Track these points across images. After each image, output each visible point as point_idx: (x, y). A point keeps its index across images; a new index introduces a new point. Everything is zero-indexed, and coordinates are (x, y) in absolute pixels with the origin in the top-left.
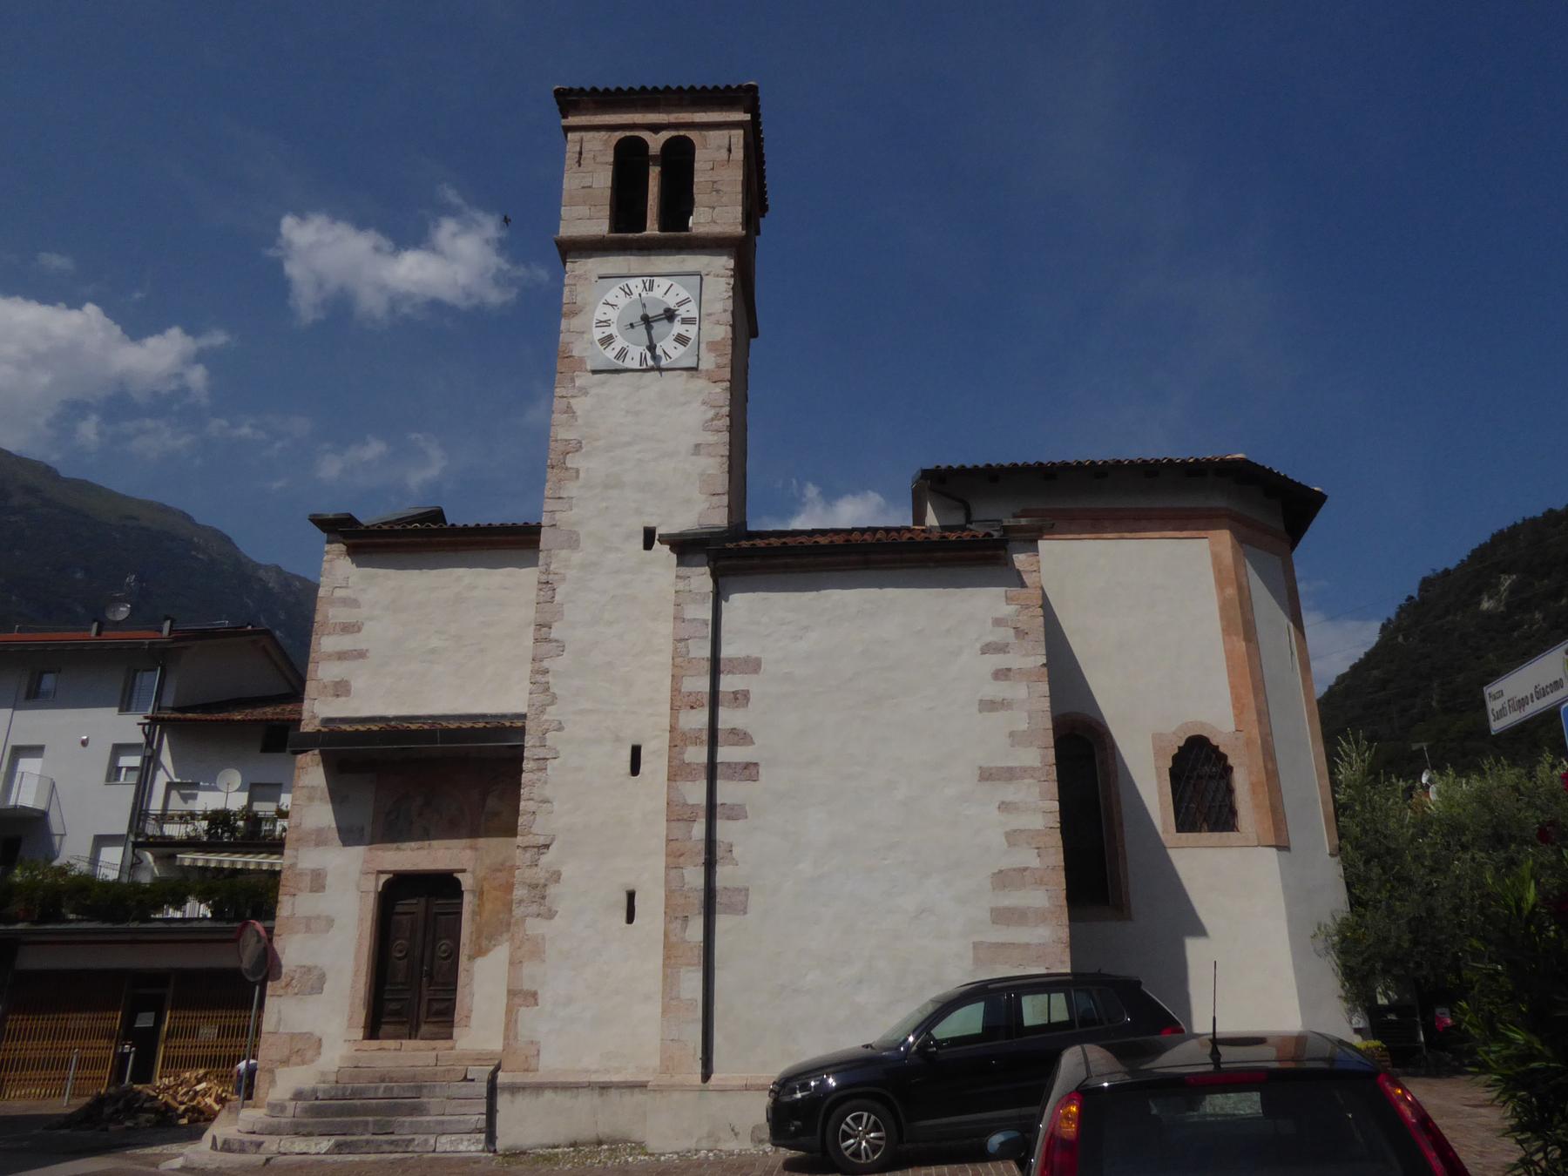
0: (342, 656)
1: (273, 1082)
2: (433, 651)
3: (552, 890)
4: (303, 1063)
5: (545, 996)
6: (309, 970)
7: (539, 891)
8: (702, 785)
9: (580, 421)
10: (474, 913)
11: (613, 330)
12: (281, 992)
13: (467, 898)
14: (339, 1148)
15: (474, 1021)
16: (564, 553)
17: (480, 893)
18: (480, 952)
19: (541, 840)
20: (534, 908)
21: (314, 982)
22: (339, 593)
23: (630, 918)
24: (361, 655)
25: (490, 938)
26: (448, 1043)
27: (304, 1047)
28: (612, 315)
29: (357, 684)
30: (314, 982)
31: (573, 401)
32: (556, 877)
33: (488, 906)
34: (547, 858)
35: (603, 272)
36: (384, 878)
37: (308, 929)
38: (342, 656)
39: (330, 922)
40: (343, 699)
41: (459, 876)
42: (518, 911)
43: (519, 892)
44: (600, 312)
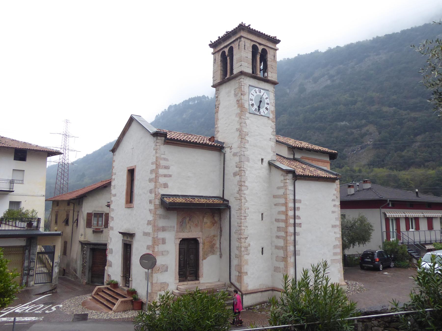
0: (165, 176)
2: (189, 177)
3: (249, 248)
5: (249, 273)
7: (246, 248)
8: (293, 228)
9: (248, 127)
10: (203, 249)
11: (253, 102)
12: (157, 272)
16: (247, 163)
17: (204, 244)
18: (204, 258)
19: (246, 236)
20: (246, 253)
21: (165, 269)
22: (163, 156)
23: (262, 254)
24: (170, 176)
25: (207, 255)
26: (197, 282)
28: (253, 98)
29: (170, 185)
30: (165, 269)
32: (249, 245)
33: (206, 247)
34: (247, 241)
35: (251, 84)
36: (180, 240)
37: (163, 255)
38: (165, 176)
39: (168, 252)
41: (198, 239)
42: (243, 253)
43: (243, 249)
44: (251, 97)
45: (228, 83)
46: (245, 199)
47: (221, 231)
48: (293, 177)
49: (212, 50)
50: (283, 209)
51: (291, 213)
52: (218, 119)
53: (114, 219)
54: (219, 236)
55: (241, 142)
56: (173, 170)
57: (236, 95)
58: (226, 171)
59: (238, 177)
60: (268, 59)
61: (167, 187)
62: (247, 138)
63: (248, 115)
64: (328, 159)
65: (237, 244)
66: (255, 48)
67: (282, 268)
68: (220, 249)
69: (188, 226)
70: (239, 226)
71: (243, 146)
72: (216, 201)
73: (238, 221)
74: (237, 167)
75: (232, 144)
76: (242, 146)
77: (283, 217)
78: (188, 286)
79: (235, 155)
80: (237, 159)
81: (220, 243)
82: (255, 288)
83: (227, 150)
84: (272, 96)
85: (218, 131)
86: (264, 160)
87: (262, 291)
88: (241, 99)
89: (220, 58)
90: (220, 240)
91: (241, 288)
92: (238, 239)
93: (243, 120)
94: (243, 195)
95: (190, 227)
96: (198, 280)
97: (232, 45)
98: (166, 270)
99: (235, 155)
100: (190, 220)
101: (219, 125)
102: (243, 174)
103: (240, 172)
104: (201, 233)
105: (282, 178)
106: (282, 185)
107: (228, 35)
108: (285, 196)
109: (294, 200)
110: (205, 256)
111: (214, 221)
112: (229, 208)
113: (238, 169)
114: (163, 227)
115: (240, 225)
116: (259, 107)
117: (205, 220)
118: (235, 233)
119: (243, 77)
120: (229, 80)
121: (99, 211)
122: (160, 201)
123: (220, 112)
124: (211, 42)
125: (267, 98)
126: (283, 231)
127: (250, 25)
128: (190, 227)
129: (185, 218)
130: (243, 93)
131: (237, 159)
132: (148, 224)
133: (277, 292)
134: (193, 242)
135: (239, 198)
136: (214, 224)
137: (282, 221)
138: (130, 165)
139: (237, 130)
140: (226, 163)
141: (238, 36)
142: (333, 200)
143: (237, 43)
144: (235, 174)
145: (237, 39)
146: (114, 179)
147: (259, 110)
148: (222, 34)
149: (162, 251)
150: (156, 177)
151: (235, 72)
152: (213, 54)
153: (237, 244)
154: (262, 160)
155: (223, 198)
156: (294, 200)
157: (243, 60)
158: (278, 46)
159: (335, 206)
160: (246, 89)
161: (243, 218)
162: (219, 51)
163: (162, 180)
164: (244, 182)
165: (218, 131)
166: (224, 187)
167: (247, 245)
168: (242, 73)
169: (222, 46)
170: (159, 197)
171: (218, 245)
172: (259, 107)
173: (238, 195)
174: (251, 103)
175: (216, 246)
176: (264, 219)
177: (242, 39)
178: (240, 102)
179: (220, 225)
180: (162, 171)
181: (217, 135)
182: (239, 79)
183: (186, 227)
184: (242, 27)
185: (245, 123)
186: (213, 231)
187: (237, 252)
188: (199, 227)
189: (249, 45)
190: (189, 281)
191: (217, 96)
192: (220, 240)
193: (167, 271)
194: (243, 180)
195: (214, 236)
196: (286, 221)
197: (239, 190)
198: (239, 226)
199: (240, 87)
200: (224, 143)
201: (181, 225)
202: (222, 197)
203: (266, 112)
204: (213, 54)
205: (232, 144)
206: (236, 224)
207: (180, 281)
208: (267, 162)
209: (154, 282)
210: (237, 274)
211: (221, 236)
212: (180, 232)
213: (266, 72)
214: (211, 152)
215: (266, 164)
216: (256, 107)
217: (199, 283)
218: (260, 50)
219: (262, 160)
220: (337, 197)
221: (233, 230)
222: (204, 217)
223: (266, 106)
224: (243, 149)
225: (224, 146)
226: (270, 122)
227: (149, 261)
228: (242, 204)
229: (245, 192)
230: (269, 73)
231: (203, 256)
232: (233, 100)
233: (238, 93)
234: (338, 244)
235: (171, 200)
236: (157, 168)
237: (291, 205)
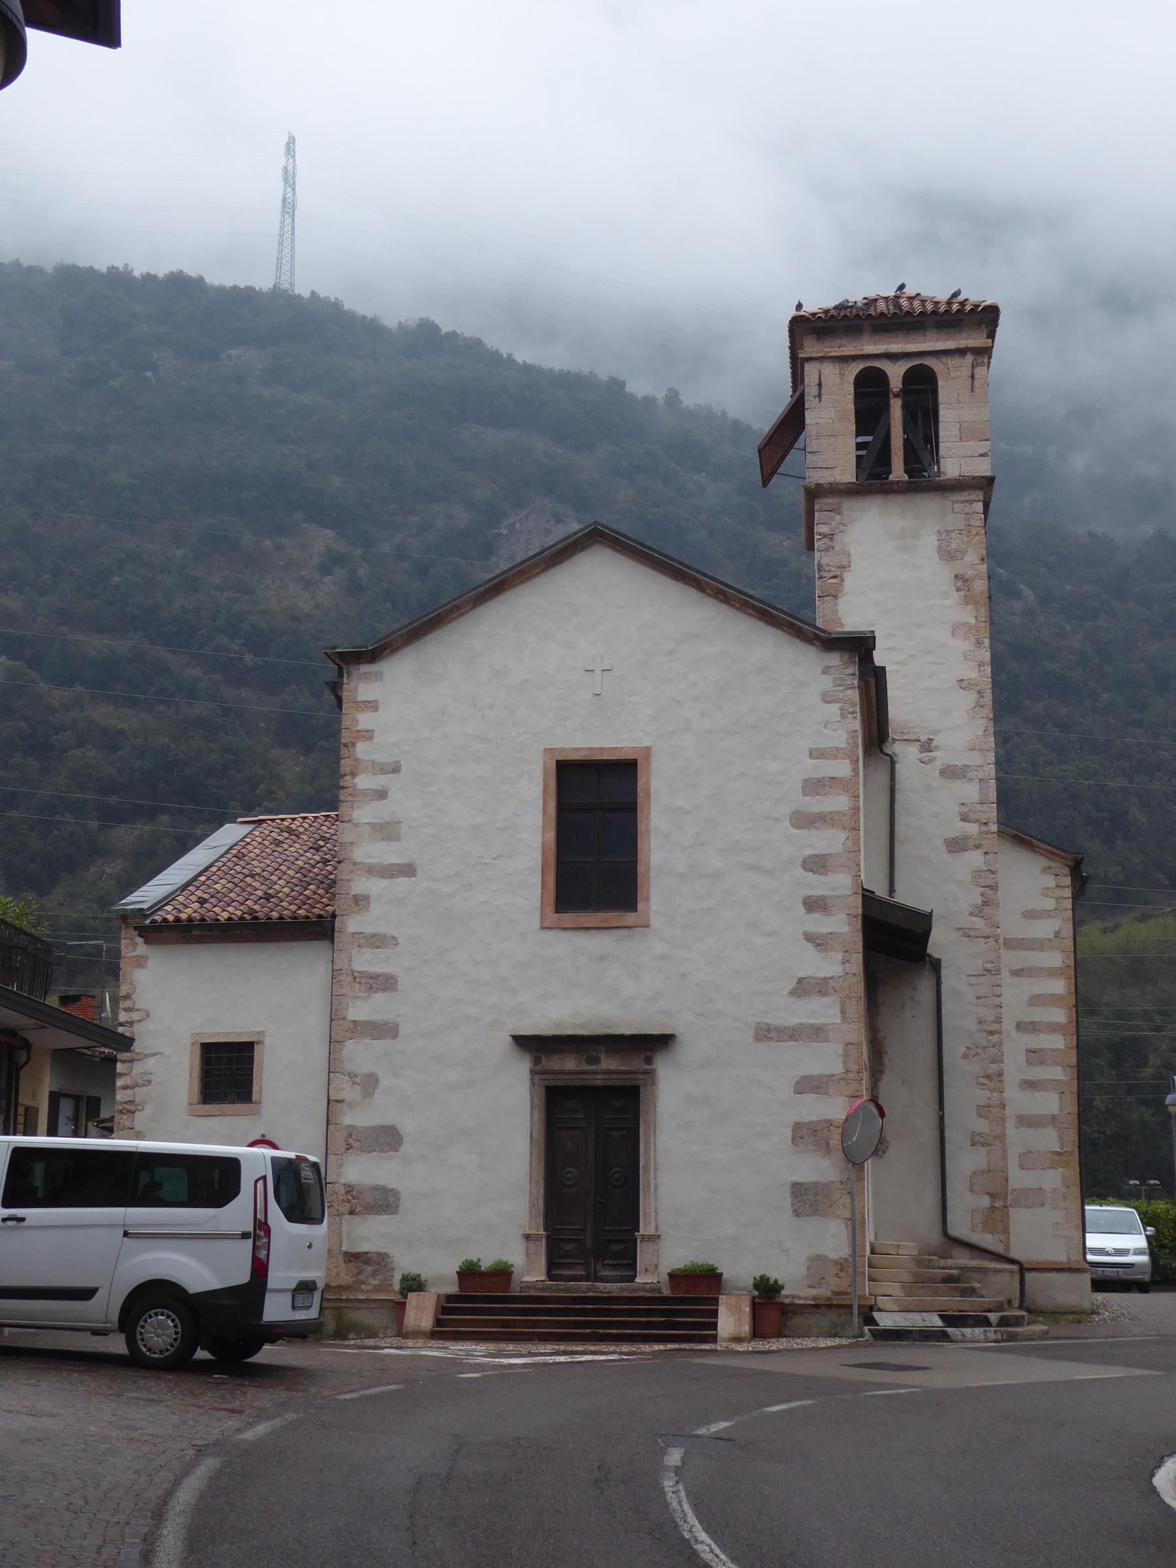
65: (982, 1096)
67: (1054, 1190)
70: (991, 1033)
74: (965, 818)
91: (1007, 1246)
92: (988, 1077)
99: (951, 773)
113: (973, 829)
115: (995, 1027)
126: (1055, 1063)
135: (987, 931)
153: (982, 1096)
173: (979, 923)
197: (986, 903)
198: (991, 1033)
206: (971, 1025)
210: (986, 1201)
221: (954, 1048)
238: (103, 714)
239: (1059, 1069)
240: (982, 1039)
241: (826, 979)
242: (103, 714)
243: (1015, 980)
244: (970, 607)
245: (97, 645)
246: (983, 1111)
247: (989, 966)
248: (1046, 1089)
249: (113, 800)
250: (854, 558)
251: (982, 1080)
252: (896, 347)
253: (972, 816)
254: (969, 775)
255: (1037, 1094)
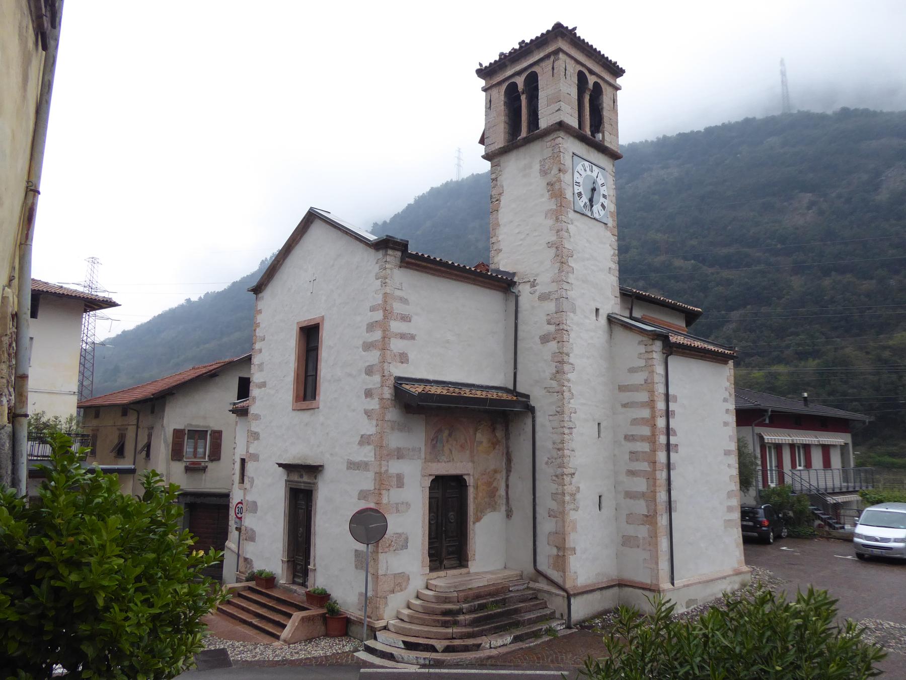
0: (403, 336)
1: (386, 604)
2: (448, 342)
3: (578, 496)
4: (402, 590)
6: (400, 535)
7: (573, 495)
9: (572, 240)
10: (475, 498)
11: (581, 189)
12: (387, 550)
13: (471, 492)
14: (517, 639)
15: (477, 557)
16: (572, 315)
17: (476, 487)
18: (478, 519)
20: (572, 506)
22: (398, 293)
24: (413, 337)
25: (482, 512)
26: (463, 571)
27: (401, 581)
28: (580, 180)
29: (411, 356)
30: (403, 543)
31: (570, 226)
34: (574, 480)
37: (398, 511)
38: (403, 336)
39: (408, 505)
40: (405, 365)
41: (466, 477)
42: (568, 507)
43: (567, 498)
45: (522, 151)
46: (570, 391)
47: (509, 460)
48: (664, 348)
49: (482, 83)
50: (646, 413)
51: (661, 423)
52: (498, 225)
53: (261, 436)
54: (504, 472)
55: (560, 270)
56: (419, 325)
57: (544, 172)
58: (520, 333)
59: (553, 345)
60: (605, 105)
61: (407, 361)
62: (571, 262)
63: (571, 215)
64: (684, 325)
65: (553, 487)
66: (582, 79)
67: (644, 538)
68: (507, 498)
69: (446, 449)
70: (559, 450)
71: (564, 278)
72: (505, 396)
73: (557, 438)
74: (549, 324)
75: (537, 275)
76: (560, 280)
77: (646, 431)
78: (447, 580)
79: (544, 297)
80: (551, 307)
81: (507, 486)
82: (589, 582)
83: (524, 290)
84: (611, 181)
85: (499, 251)
86: (601, 311)
87: (601, 589)
88: (559, 180)
89: (502, 98)
90: (507, 479)
91: (564, 581)
92: (557, 476)
93: (564, 224)
94: (566, 383)
95: (451, 451)
96: (467, 566)
97: (536, 69)
98: (405, 546)
99: (544, 297)
100: (450, 435)
101: (500, 238)
102: (565, 338)
103: (557, 333)
104: (470, 464)
105: (642, 349)
106: (642, 363)
107: (525, 49)
108: (649, 385)
109: (667, 395)
110: (479, 514)
111: (495, 440)
112: (531, 410)
113: (552, 328)
114: (399, 450)
115: (560, 446)
116: (591, 200)
117: (479, 435)
118: (547, 463)
119: (562, 134)
120: (527, 141)
121: (198, 426)
122: (391, 391)
123: (502, 211)
124: (481, 65)
125: (603, 185)
126: (645, 460)
127: (575, 29)
128: (451, 451)
129: (440, 431)
130: (562, 167)
131: (551, 307)
132: (361, 443)
133: (631, 589)
134: (453, 484)
136: (494, 444)
137: (643, 439)
138: (308, 317)
139: (550, 245)
140: (520, 316)
141: (551, 49)
142: (725, 400)
143: (548, 64)
144: (545, 339)
145: (547, 57)
146: (260, 351)
147: (592, 206)
148: (510, 45)
149: (397, 504)
150: (384, 338)
151: (543, 124)
152: (485, 90)
153: (553, 487)
154: (597, 310)
155: (514, 392)
156: (667, 395)
157: (558, 101)
158: (619, 81)
159: (727, 411)
160: (567, 160)
161: (566, 431)
162: (500, 83)
163: (397, 345)
164: (568, 354)
165: (499, 251)
166: (515, 367)
167: (574, 488)
168: (561, 126)
169: (509, 73)
170: (391, 382)
171: (502, 492)
172: (591, 200)
173: (554, 384)
174: (577, 189)
175: (497, 494)
176: (602, 435)
177: (561, 55)
178: (557, 186)
179: (508, 448)
180: (396, 326)
181: (496, 260)
182: (554, 139)
183: (443, 450)
184: (559, 31)
185: (567, 231)
186: (494, 461)
187: (553, 505)
188: (468, 452)
189: (573, 69)
190: (446, 568)
191: (494, 176)
192: (507, 479)
193: (406, 547)
194: (565, 350)
195: (495, 471)
196: (652, 439)
197: (557, 372)
198: (559, 450)
199: (556, 156)
200: (514, 274)
201: (434, 447)
202: (511, 387)
203: (602, 213)
204: (485, 90)
205: (537, 275)
206: (550, 445)
207: (432, 569)
208: (605, 317)
209: (381, 572)
210: (554, 551)
211: (509, 470)
212: (432, 461)
213: (598, 132)
214: (487, 291)
215: (603, 320)
216: (585, 199)
217: (469, 573)
218: (591, 85)
219: (597, 310)
220: (730, 395)
222: (476, 430)
223: (602, 200)
224: (565, 286)
225: (516, 279)
226: (609, 234)
227: (369, 526)
228: (566, 401)
229: (569, 376)
230: (606, 134)
231: (476, 514)
232: (537, 183)
233: (551, 169)
234: (734, 488)
235: (418, 389)
236: (385, 317)
237: (661, 405)
238: (726, 274)
239: (646, 464)
240: (554, 453)
241: (370, 435)
242: (726, 274)
243: (624, 409)
244: (553, 200)
245: (725, 251)
246: (554, 495)
247: (558, 409)
248: (639, 476)
249: (730, 303)
250: (505, 188)
251: (554, 478)
252: (518, 68)
253: (553, 321)
254: (551, 297)
255: (635, 479)
